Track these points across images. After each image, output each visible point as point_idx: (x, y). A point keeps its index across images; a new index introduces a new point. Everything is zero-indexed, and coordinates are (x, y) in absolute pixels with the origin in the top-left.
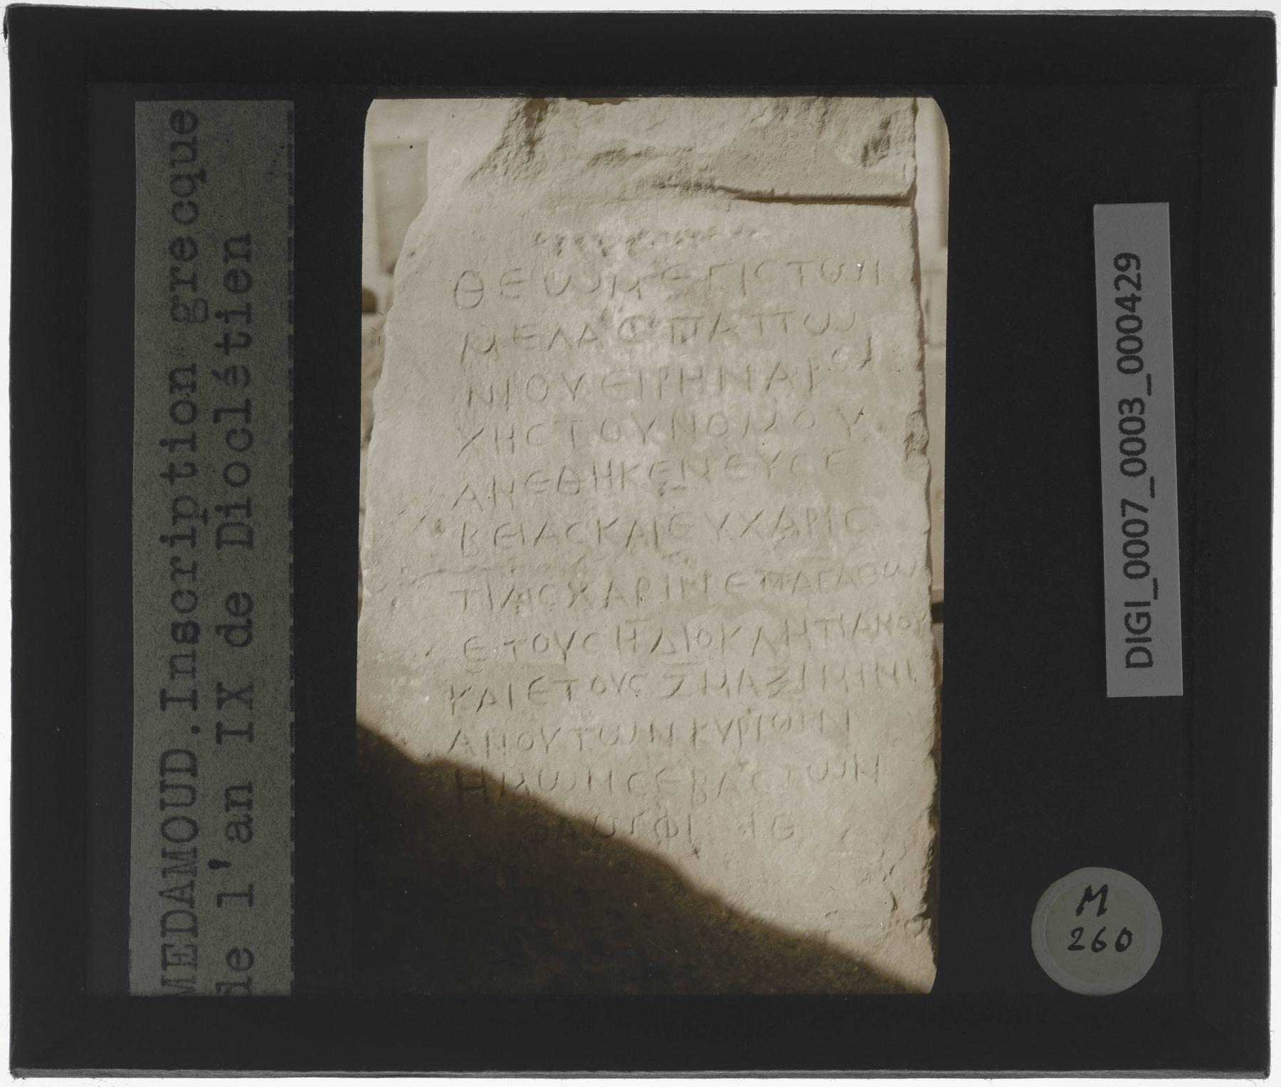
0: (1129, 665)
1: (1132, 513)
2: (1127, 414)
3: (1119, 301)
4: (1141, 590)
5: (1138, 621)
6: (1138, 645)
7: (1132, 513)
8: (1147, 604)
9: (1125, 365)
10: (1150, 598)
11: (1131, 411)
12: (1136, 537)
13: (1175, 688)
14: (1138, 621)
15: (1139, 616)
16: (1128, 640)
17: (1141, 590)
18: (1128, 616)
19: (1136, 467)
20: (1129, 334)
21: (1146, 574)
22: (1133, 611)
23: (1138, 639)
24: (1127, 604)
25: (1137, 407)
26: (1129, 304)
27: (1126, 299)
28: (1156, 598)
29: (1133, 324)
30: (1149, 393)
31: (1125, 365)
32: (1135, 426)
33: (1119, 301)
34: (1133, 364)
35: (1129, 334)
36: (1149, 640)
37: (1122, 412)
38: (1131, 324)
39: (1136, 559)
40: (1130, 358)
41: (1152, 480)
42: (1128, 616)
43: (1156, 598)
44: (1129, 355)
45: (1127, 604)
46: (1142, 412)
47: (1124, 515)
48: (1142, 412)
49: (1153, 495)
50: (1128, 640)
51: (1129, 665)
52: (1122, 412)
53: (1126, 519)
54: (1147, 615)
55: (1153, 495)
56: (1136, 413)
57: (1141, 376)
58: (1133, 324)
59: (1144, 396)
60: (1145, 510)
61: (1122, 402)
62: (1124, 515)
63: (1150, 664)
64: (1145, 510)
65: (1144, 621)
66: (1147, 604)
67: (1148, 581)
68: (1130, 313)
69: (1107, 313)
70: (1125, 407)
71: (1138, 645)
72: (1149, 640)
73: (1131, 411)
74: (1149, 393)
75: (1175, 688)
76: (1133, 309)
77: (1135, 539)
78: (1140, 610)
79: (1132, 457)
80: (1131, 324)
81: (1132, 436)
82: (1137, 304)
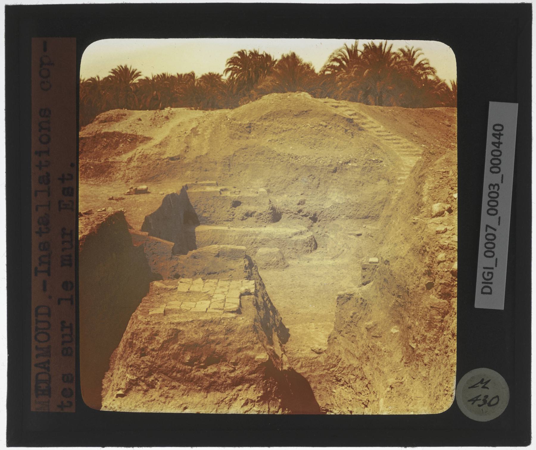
0: (482, 293)
1: (490, 231)
2: (492, 190)
3: (493, 143)
4: (490, 263)
5: (488, 275)
6: (486, 285)
7: (490, 231)
8: (492, 268)
9: (493, 170)
10: (494, 266)
11: (494, 189)
12: (491, 240)
13: (500, 306)
14: (488, 275)
15: (489, 273)
16: (483, 283)
17: (490, 263)
18: (484, 273)
19: (493, 212)
20: (496, 157)
21: (492, 257)
22: (487, 271)
23: (488, 282)
24: (484, 268)
25: (496, 187)
26: (497, 145)
27: (497, 143)
28: (496, 266)
29: (498, 153)
30: (502, 182)
31: (493, 170)
32: (494, 195)
33: (493, 143)
34: (496, 170)
35: (496, 157)
36: (491, 283)
37: (490, 189)
38: (497, 153)
39: (489, 250)
40: (496, 167)
41: (499, 218)
42: (484, 273)
43: (496, 266)
44: (495, 166)
45: (484, 268)
46: (498, 190)
47: (486, 231)
48: (498, 190)
49: (499, 225)
50: (483, 283)
51: (482, 293)
52: (490, 189)
53: (486, 233)
54: (492, 273)
55: (499, 225)
56: (496, 190)
57: (500, 175)
58: (498, 153)
59: (501, 185)
60: (495, 230)
61: (491, 185)
62: (486, 231)
63: (490, 293)
64: (495, 230)
65: (490, 275)
66: (492, 268)
67: (494, 259)
68: (496, 148)
69: (489, 148)
70: (492, 187)
71: (486, 285)
72: (491, 283)
73: (494, 189)
74: (502, 182)
75: (500, 306)
76: (498, 147)
77: (490, 241)
78: (490, 270)
79: (492, 208)
80: (497, 153)
81: (493, 199)
82: (501, 145)
